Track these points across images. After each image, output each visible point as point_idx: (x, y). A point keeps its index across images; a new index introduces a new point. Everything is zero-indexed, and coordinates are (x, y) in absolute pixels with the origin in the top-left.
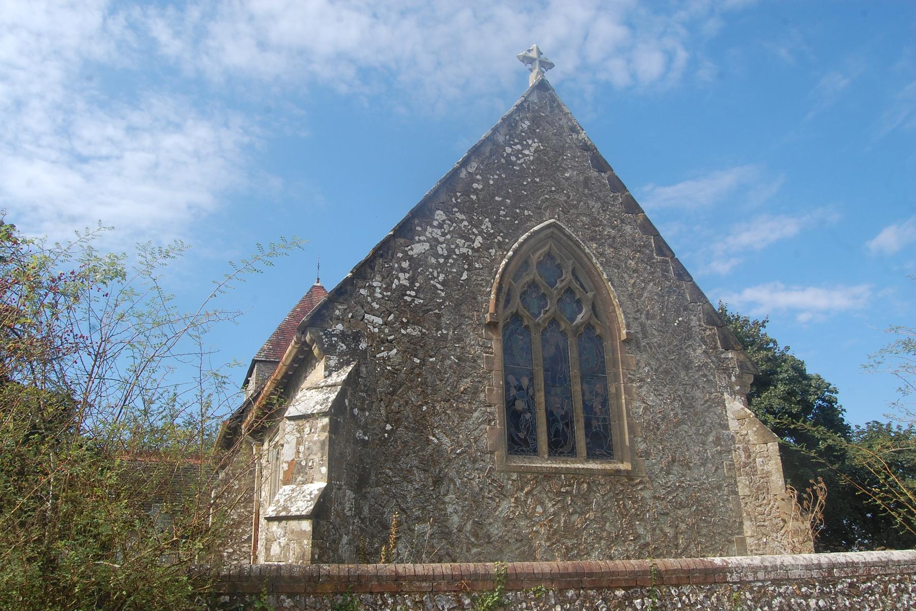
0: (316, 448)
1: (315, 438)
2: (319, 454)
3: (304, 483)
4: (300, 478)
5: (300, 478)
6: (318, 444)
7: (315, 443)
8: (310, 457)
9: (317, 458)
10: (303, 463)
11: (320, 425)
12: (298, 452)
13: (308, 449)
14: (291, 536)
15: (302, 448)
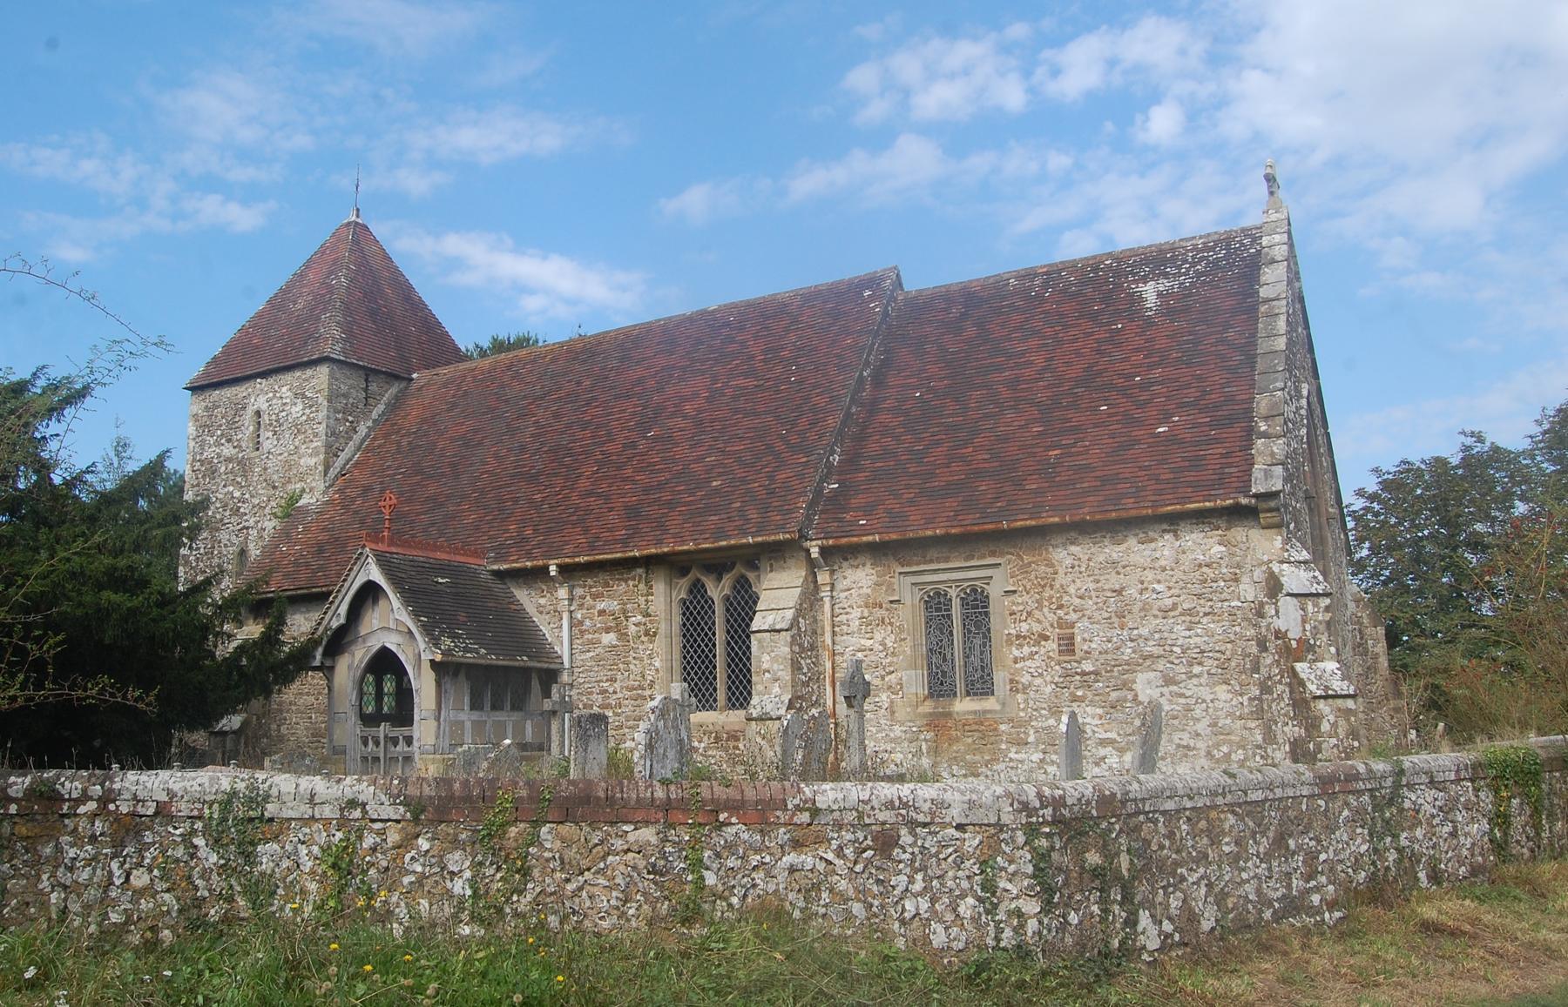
0: (1322, 628)
1: (1320, 617)
2: (1326, 634)
3: (1314, 661)
4: (1310, 657)
5: (1310, 657)
6: (1324, 624)
7: (1320, 622)
8: (1318, 636)
9: (1324, 638)
10: (1312, 642)
11: (1323, 605)
12: (1305, 630)
13: (1315, 627)
14: (1338, 714)
15: (1308, 627)
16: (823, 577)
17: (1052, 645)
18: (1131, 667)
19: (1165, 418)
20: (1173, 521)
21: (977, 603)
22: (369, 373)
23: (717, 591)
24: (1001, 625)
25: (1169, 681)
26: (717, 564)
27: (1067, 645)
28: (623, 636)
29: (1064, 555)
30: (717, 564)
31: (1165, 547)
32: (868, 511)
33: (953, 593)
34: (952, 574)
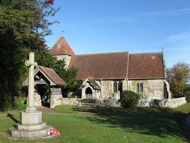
16: (128, 82)
17: (148, 88)
18: (154, 90)
19: (157, 70)
20: (158, 79)
21: (142, 84)
22: (69, 55)
23: (118, 82)
24: (144, 86)
25: (157, 91)
26: (117, 80)
27: (149, 88)
28: (108, 86)
29: (149, 81)
30: (117, 80)
31: (157, 81)
32: (132, 76)
33: (139, 84)
34: (140, 82)
